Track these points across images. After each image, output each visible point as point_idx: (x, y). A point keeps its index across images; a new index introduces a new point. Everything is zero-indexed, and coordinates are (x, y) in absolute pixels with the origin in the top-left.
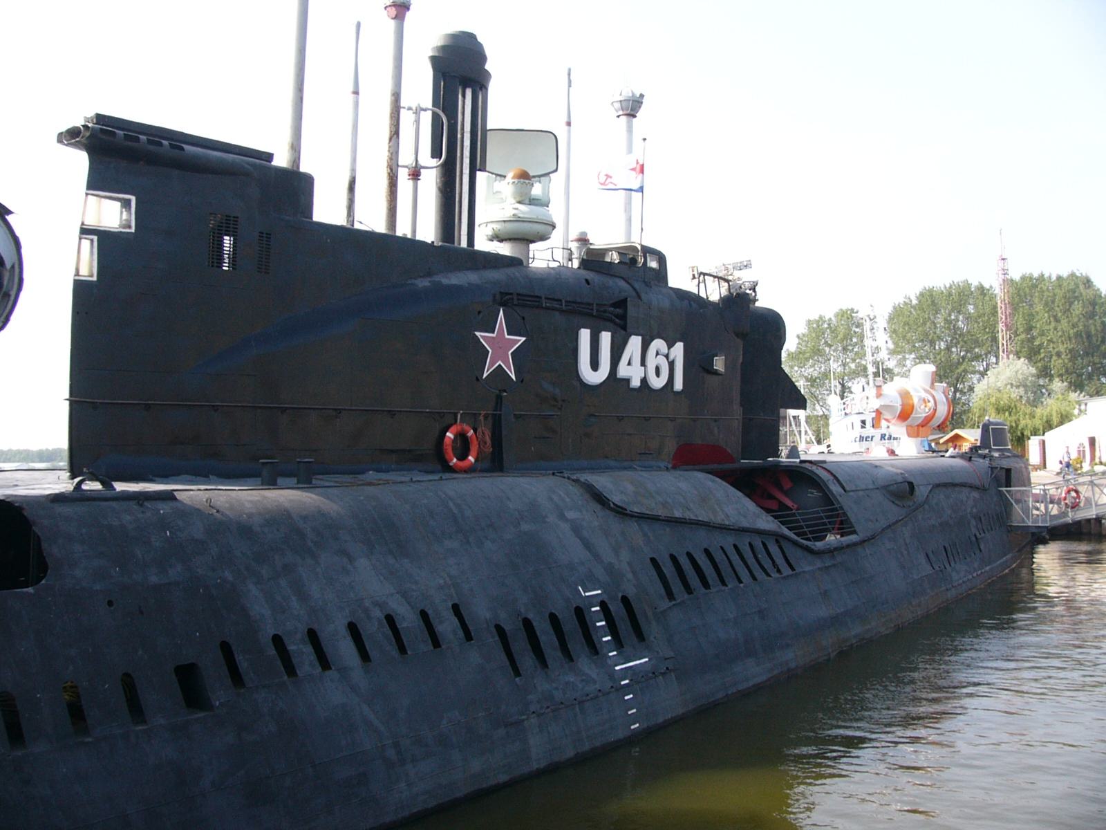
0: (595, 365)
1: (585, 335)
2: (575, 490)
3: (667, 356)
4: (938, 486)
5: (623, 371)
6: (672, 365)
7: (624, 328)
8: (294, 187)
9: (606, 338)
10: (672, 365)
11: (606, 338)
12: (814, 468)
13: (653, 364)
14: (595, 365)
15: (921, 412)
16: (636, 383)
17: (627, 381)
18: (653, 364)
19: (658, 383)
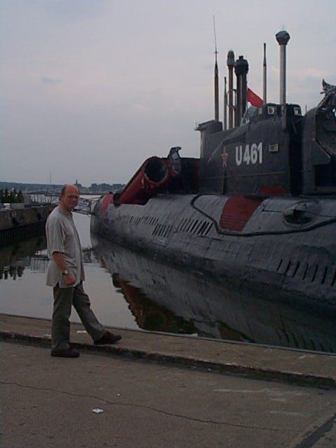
0: (239, 159)
1: (237, 148)
5: (245, 159)
9: (241, 147)
14: (239, 159)
16: (248, 163)
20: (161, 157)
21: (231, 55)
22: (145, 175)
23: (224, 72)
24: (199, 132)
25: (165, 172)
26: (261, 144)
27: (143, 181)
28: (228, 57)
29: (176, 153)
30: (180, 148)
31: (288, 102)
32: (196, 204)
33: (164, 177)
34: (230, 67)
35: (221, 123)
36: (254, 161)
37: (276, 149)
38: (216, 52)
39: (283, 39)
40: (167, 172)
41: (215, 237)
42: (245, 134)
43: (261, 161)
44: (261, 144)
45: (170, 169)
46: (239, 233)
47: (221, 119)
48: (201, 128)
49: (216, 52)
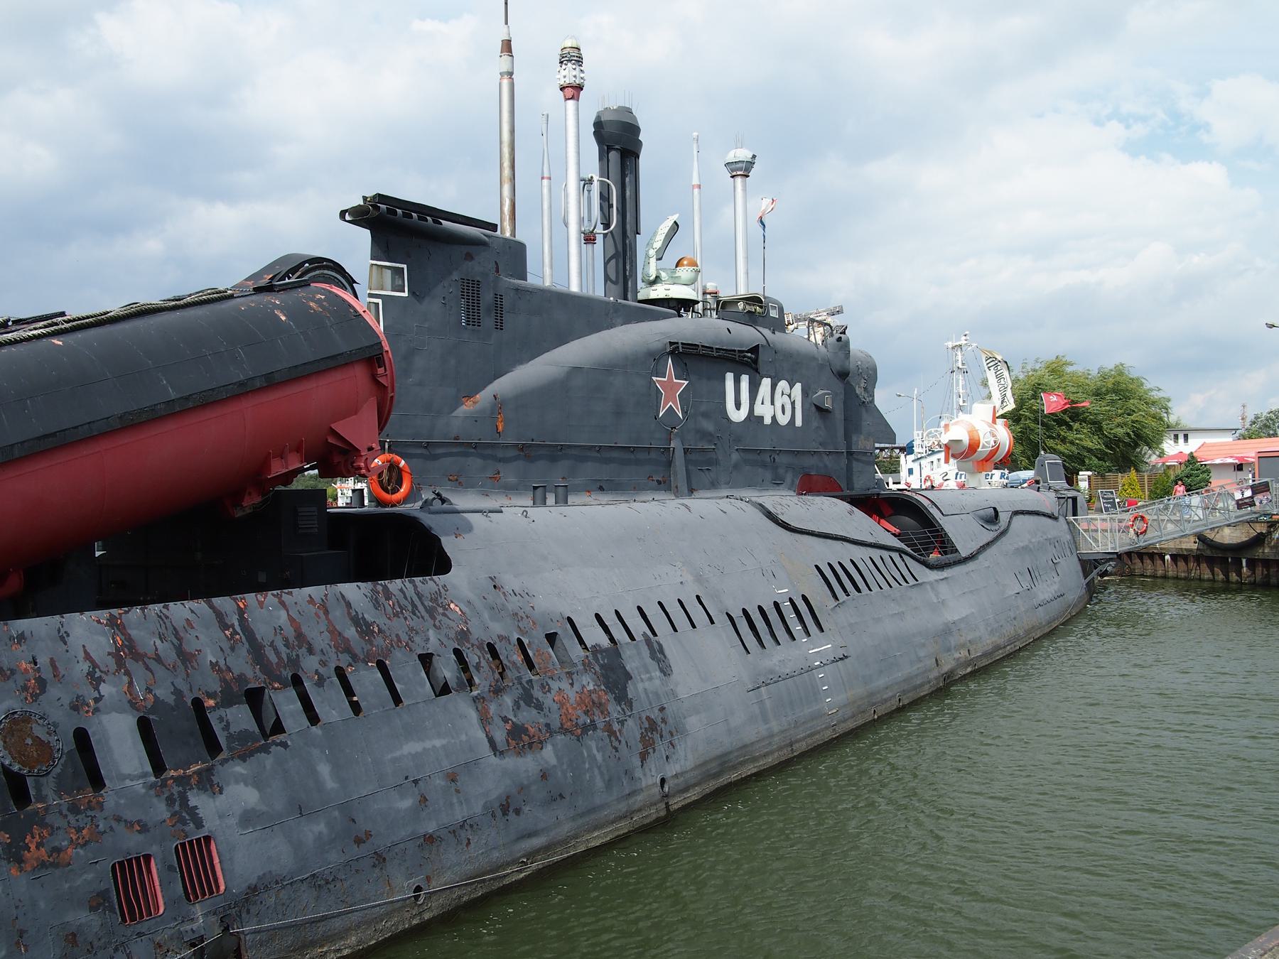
0: (738, 405)
1: (730, 377)
2: (749, 508)
3: (789, 396)
4: (1016, 513)
5: (758, 410)
6: (793, 403)
8: (515, 254)
9: (745, 380)
10: (793, 403)
11: (745, 380)
12: (914, 495)
13: (778, 403)
14: (738, 405)
15: (983, 450)
16: (768, 421)
18: (778, 403)
19: (783, 420)
24: (365, 234)
26: (798, 386)
36: (783, 420)
42: (755, 350)
43: (799, 423)
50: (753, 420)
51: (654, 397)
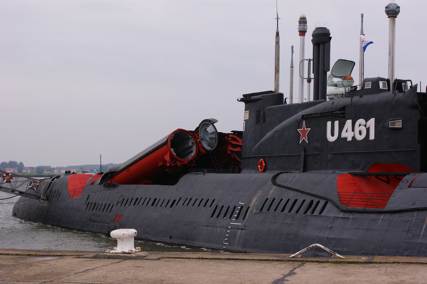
0: (333, 135)
1: (329, 124)
3: (365, 126)
5: (344, 135)
6: (368, 130)
7: (344, 117)
9: (337, 123)
10: (368, 130)
14: (333, 135)
17: (346, 138)
19: (360, 138)
20: (187, 130)
21: (303, 21)
22: (172, 149)
23: (290, 37)
24: (243, 104)
25: (191, 147)
27: (167, 157)
28: (300, 22)
29: (211, 126)
30: (215, 121)
31: (398, 76)
32: (278, 181)
33: (192, 151)
34: (302, 33)
35: (281, 95)
37: (399, 124)
38: (278, 17)
39: (392, 12)
40: (194, 148)
41: (337, 215)
44: (372, 122)
45: (199, 145)
46: (383, 210)
47: (284, 90)
48: (248, 99)
49: (278, 17)
50: (341, 140)
51: (298, 136)
